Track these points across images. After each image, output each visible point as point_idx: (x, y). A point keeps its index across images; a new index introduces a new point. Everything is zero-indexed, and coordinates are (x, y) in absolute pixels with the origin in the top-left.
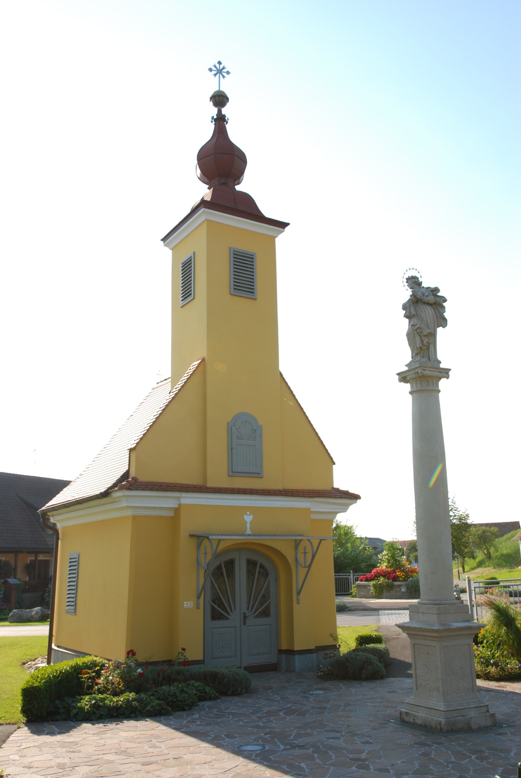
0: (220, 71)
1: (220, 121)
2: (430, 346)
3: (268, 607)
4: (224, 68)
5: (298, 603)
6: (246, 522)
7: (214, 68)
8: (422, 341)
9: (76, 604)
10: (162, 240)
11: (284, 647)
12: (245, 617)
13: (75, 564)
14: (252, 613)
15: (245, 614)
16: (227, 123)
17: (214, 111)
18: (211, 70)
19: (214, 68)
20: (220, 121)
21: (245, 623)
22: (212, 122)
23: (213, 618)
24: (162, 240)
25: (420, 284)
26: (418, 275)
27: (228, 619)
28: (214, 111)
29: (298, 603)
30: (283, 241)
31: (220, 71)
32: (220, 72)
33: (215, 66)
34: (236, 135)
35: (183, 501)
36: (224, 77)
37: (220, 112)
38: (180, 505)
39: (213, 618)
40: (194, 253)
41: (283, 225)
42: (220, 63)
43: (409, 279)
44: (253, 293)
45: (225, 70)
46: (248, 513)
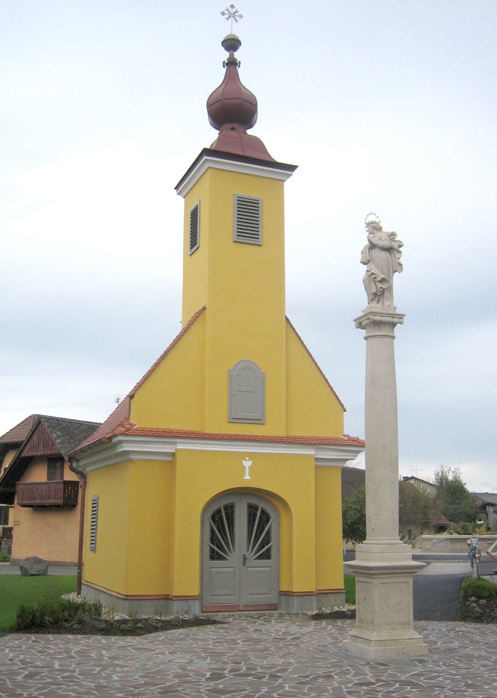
0: (232, 14)
1: (232, 64)
2: (385, 292)
3: (269, 550)
4: (236, 12)
5: (93, 550)
6: (245, 468)
7: (226, 12)
8: (377, 287)
9: (96, 543)
10: (175, 188)
11: (284, 589)
12: (245, 559)
13: (95, 504)
14: (252, 555)
15: (244, 556)
16: (239, 67)
17: (225, 55)
18: (223, 14)
19: (226, 12)
20: (232, 64)
21: (244, 564)
22: (224, 67)
23: (212, 558)
24: (175, 188)
25: (380, 229)
26: (377, 221)
27: (224, 558)
28: (225, 55)
29: (93, 550)
30: (291, 185)
31: (232, 14)
32: (232, 15)
33: (228, 10)
34: (248, 78)
35: (179, 446)
36: (236, 21)
37: (232, 56)
38: (176, 450)
39: (212, 558)
40: (200, 201)
41: (292, 168)
42: (232, 6)
43: (368, 224)
44: (258, 238)
45: (226, 16)
46: (247, 459)
